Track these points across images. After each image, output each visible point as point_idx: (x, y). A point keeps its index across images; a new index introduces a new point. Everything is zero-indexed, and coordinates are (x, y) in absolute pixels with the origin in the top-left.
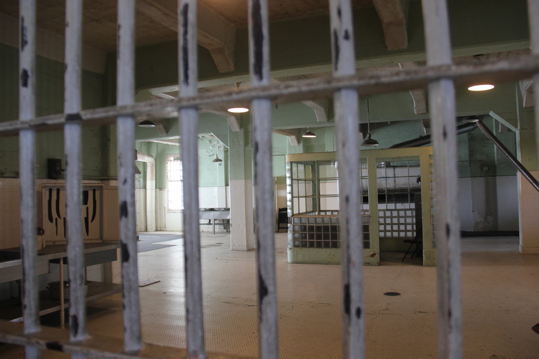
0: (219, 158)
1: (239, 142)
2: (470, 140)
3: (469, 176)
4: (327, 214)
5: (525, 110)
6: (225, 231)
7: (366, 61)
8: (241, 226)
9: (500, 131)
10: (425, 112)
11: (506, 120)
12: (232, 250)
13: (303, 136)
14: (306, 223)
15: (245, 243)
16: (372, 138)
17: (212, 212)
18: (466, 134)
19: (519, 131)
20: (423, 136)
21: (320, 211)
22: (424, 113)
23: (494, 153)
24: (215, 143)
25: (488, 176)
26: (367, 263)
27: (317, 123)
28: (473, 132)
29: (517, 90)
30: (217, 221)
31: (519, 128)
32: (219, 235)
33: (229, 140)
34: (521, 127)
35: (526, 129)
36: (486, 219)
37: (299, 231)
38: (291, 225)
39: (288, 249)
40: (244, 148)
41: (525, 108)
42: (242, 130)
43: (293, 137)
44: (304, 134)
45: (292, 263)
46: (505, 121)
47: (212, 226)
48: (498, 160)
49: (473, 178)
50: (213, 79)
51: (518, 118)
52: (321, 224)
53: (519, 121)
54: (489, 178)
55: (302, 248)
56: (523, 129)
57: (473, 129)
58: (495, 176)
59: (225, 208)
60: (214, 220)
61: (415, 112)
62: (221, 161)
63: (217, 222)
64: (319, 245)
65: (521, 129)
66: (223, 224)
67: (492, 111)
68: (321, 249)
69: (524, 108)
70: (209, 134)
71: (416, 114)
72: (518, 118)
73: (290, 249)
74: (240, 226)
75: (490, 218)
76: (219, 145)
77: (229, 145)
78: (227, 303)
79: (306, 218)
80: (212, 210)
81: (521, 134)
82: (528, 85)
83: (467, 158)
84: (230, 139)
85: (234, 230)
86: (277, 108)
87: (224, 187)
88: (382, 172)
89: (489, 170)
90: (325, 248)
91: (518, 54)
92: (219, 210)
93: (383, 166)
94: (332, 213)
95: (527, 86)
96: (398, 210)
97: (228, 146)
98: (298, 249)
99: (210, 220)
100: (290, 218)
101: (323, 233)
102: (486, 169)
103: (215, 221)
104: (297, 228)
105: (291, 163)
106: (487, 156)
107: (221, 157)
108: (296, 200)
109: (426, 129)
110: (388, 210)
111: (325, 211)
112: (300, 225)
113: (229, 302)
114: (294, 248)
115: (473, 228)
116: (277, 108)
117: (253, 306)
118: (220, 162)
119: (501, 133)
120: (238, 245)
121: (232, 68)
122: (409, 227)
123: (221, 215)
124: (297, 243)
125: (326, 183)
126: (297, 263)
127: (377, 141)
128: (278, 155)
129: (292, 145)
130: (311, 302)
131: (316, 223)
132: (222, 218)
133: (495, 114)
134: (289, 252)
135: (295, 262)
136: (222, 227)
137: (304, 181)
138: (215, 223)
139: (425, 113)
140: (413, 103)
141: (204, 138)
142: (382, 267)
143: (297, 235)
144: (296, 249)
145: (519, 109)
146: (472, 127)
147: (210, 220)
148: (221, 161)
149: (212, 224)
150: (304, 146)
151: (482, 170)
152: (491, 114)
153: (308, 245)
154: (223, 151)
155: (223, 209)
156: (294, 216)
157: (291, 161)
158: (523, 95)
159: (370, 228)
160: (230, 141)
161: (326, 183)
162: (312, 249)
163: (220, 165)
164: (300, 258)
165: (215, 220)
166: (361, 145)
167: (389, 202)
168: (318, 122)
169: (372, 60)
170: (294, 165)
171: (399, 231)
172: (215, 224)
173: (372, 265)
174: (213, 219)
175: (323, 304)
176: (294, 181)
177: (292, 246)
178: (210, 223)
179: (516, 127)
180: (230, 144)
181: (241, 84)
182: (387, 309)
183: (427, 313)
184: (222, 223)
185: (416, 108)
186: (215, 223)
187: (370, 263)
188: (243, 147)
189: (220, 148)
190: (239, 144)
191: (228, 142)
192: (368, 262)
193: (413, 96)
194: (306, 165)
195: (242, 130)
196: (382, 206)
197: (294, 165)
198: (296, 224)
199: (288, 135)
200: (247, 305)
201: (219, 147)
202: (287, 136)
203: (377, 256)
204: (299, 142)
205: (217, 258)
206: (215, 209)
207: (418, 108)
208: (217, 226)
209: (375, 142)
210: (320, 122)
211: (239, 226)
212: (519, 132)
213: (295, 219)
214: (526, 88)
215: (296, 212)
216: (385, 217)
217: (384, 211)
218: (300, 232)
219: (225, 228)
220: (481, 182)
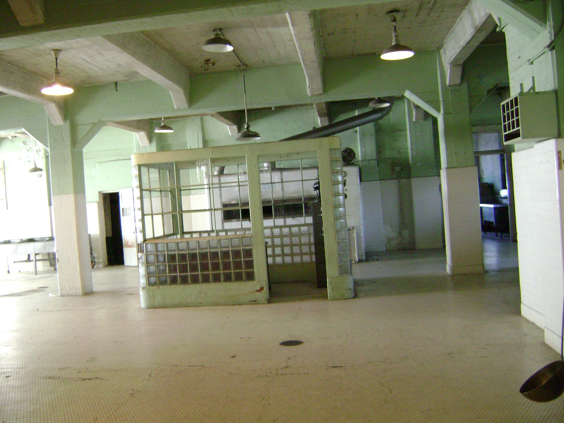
0: (38, 166)
1: (64, 140)
2: (378, 132)
3: (378, 179)
4: (194, 236)
5: (449, 89)
6: (52, 268)
7: (243, 7)
8: (72, 261)
9: (414, 119)
10: (321, 92)
11: (426, 102)
12: (61, 296)
14: (164, 251)
15: (79, 284)
16: (252, 129)
17: (32, 244)
18: (372, 124)
19: (442, 116)
20: (317, 127)
21: (183, 233)
22: (320, 93)
23: (407, 149)
24: (31, 145)
25: (401, 178)
26: (252, 301)
28: (380, 122)
29: (438, 63)
30: (40, 255)
31: (442, 112)
32: (43, 275)
34: (444, 110)
35: (451, 113)
36: (400, 233)
37: (155, 263)
38: (143, 254)
39: (140, 288)
40: (72, 149)
41: (449, 86)
42: (68, 122)
43: (143, 134)
44: (157, 128)
45: (148, 308)
47: (32, 264)
48: (412, 158)
49: (382, 182)
50: (9, 36)
51: (441, 99)
52: (185, 250)
53: (441, 103)
54: (402, 180)
55: (161, 287)
57: (381, 118)
58: (409, 178)
59: (51, 237)
60: (34, 255)
61: (309, 93)
62: (41, 170)
63: (38, 257)
64: (184, 281)
65: (446, 114)
66: (49, 259)
67: (407, 89)
68: (187, 286)
70: (19, 131)
71: (310, 95)
72: (441, 99)
73: (144, 288)
74: (71, 262)
75: (406, 233)
76: (37, 148)
77: (49, 144)
78: (49, 378)
79: (164, 243)
80: (31, 240)
81: (445, 121)
82: (453, 55)
83: (374, 156)
84: (50, 137)
85: (62, 266)
86: (117, 91)
87: (48, 207)
88: (266, 177)
89: (402, 169)
90: (193, 283)
91: (442, 11)
92: (42, 240)
93: (266, 168)
94: (200, 235)
95: (451, 57)
96: (290, 227)
97: (47, 147)
98: (155, 287)
99: (29, 255)
100: (141, 245)
101: (188, 263)
102: (398, 169)
103: (36, 256)
104: (152, 258)
105: (140, 166)
106: (399, 153)
107: (41, 164)
108: (148, 219)
110: (275, 227)
111: (191, 233)
112: (156, 253)
113: (53, 377)
114: (149, 286)
115: (384, 246)
116: (117, 91)
117: (89, 379)
118: (40, 172)
119: (415, 122)
120: (69, 288)
121: (40, 18)
122: (305, 249)
123: (44, 247)
124: (153, 280)
125: (191, 196)
126: (155, 308)
127: (258, 134)
128: (122, 160)
129: (141, 145)
130: (176, 366)
131: (178, 250)
132: (47, 251)
133: (412, 94)
134: (142, 293)
135: (152, 306)
136: (47, 263)
137: (160, 192)
138: (37, 259)
139: (321, 94)
140: (305, 80)
141: (15, 138)
142: (273, 306)
143: (152, 268)
144: (151, 288)
145: (442, 87)
146: (379, 115)
147: (29, 255)
148: (41, 170)
149: (32, 261)
150: (157, 145)
151: (393, 170)
152: (407, 94)
153: (169, 281)
154: (44, 156)
155: (48, 239)
156: (145, 242)
157: (139, 164)
158: (445, 69)
159: (254, 253)
161: (190, 195)
162: (174, 287)
163: (40, 176)
164: (158, 300)
165: (36, 254)
166: (236, 140)
167: (276, 216)
168: (176, 109)
169: (252, 6)
170: (144, 170)
171: (292, 255)
172: (36, 260)
173: (259, 304)
174: (34, 253)
175: (194, 366)
176: (144, 192)
177: (146, 285)
178: (29, 260)
179: (439, 111)
180: (50, 143)
181: (61, 53)
182: (287, 367)
183: (344, 367)
184: (47, 258)
185: (309, 88)
186: (37, 259)
187: (256, 301)
188: (70, 147)
189: (40, 152)
192: (254, 299)
193: (306, 69)
194: (160, 170)
196: (269, 222)
197: (144, 170)
198: (151, 252)
199: (135, 131)
200: (80, 378)
201: (37, 151)
202: (134, 133)
203: (266, 290)
204: (150, 140)
205: (38, 310)
206: (36, 239)
208: (39, 264)
209: (256, 135)
210: (179, 110)
211: (69, 261)
212: (442, 117)
213: (149, 246)
214: (450, 60)
215: (149, 235)
216: (273, 237)
217: (271, 228)
218: (156, 264)
219: (51, 265)
220: (392, 186)
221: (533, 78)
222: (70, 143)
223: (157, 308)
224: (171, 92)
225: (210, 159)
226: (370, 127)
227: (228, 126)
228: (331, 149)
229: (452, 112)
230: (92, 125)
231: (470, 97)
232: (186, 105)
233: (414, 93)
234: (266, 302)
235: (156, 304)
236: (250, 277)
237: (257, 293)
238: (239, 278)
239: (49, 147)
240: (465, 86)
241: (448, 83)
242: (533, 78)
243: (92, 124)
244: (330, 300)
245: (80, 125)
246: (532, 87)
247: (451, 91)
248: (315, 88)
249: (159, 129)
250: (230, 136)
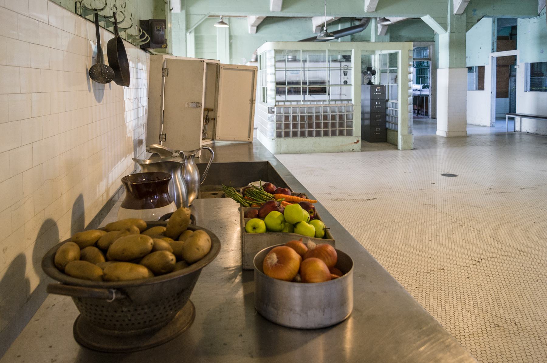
9: (379, 34)
11: (439, 24)
22: (373, 11)
41: (455, 15)
42: (184, 11)
46: (438, 25)
51: (449, 22)
56: (452, 33)
65: (451, 32)
68: (305, 138)
72: (449, 22)
119: (379, 36)
133: (431, 18)
173: (355, 152)
179: (446, 30)
190: (179, 27)
222: (185, 28)
223: (283, 154)
226: (349, 37)
228: (409, 50)
229: (455, 32)
231: (467, 23)
232: (280, 9)
233: (432, 17)
234: (360, 151)
235: (282, 151)
236: (350, 133)
237: (354, 144)
238: (341, 134)
240: (465, 15)
241: (455, 12)
244: (403, 150)
245: (193, 15)
247: (456, 18)
250: (249, 34)
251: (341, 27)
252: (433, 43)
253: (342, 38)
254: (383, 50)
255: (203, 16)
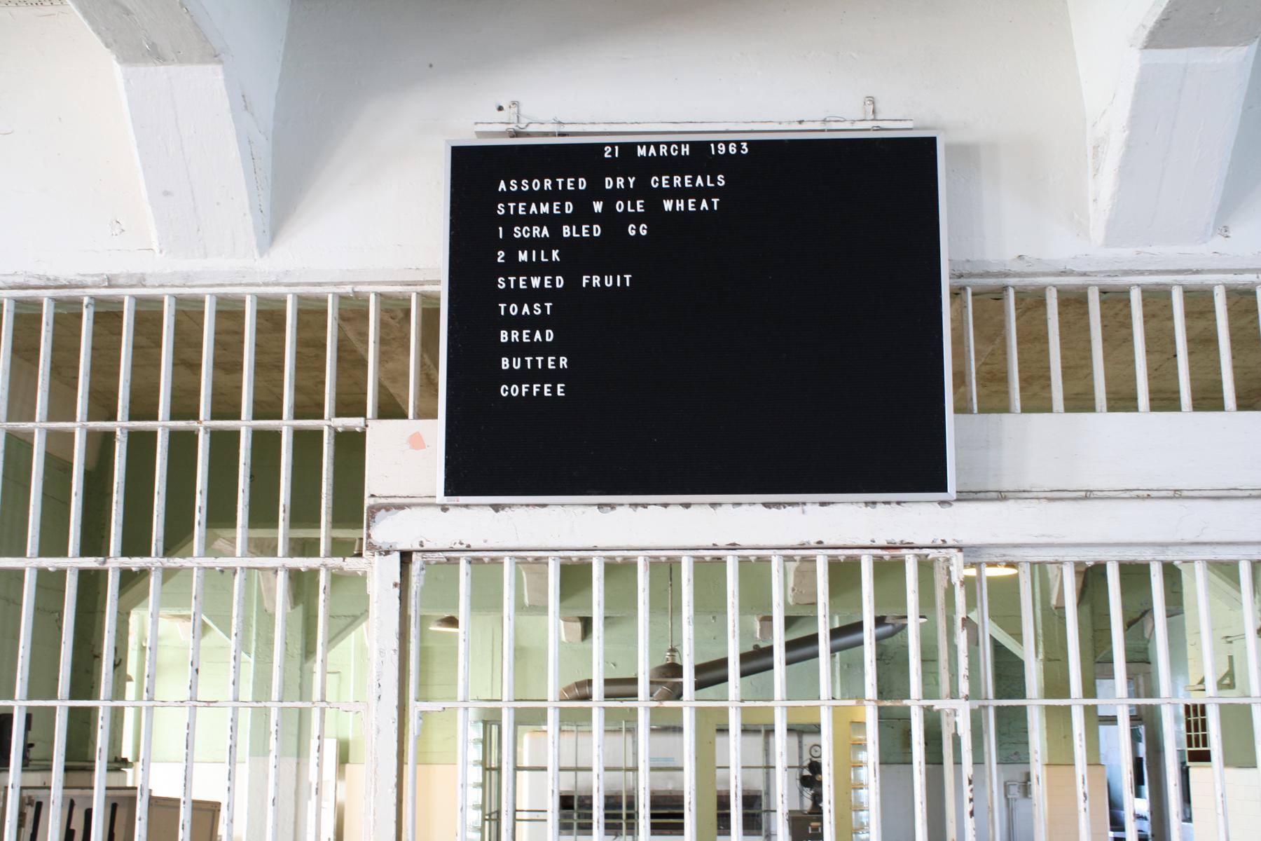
11: (1011, 635)
13: (431, 628)
19: (1042, 663)
27: (522, 608)
33: (254, 637)
35: (1059, 660)
40: (302, 664)
41: (1056, 608)
42: (300, 608)
46: (1009, 637)
56: (1050, 660)
69: (1053, 608)
84: (258, 634)
109: (761, 625)
160: (257, 640)
168: (527, 606)
180: (257, 648)
185: (793, 590)
191: (251, 642)
195: (300, 608)
207: (798, 590)
212: (1042, 666)
221: (1231, 658)
222: (300, 651)
224: (527, 573)
225: (626, 722)
227: (562, 622)
230: (349, 620)
231: (1094, 631)
239: (253, 655)
242: (1231, 658)
243: (349, 616)
246: (1228, 672)
248: (804, 592)
249: (440, 625)
251: (840, 620)
252: (1147, 665)
253: (844, 652)
254: (903, 699)
255: (349, 620)
